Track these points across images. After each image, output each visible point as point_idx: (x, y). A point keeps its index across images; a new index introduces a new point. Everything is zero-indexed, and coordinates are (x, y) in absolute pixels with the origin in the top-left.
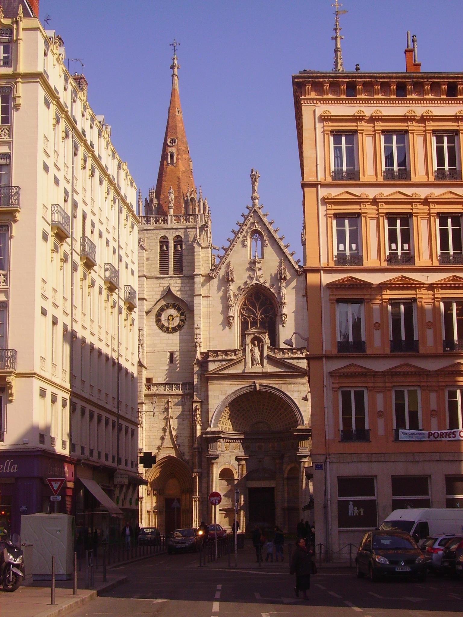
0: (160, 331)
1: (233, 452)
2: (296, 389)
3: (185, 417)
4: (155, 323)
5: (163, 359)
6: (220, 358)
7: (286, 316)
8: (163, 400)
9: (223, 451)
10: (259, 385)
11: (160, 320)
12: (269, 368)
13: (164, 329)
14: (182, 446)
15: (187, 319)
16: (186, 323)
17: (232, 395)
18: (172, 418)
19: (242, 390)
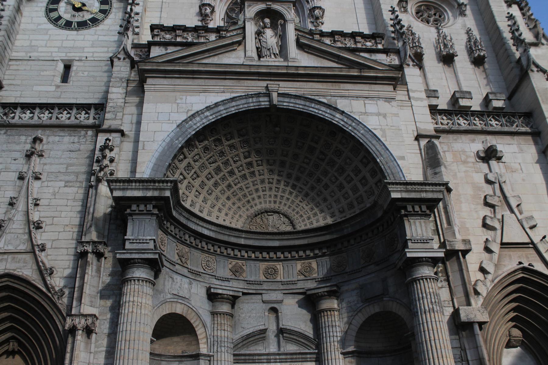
0: (51, 26)
1: (198, 274)
2: (371, 107)
3: (72, 177)
4: (42, 13)
5: (45, 73)
6: (179, 39)
7: (323, 11)
8: (23, 138)
9: (173, 264)
10: (280, 95)
11: (56, 10)
12: (304, 60)
13: (60, 23)
14: (48, 251)
15: (113, 10)
16: (111, 16)
17: (208, 113)
18: (37, 178)
19: (234, 104)
